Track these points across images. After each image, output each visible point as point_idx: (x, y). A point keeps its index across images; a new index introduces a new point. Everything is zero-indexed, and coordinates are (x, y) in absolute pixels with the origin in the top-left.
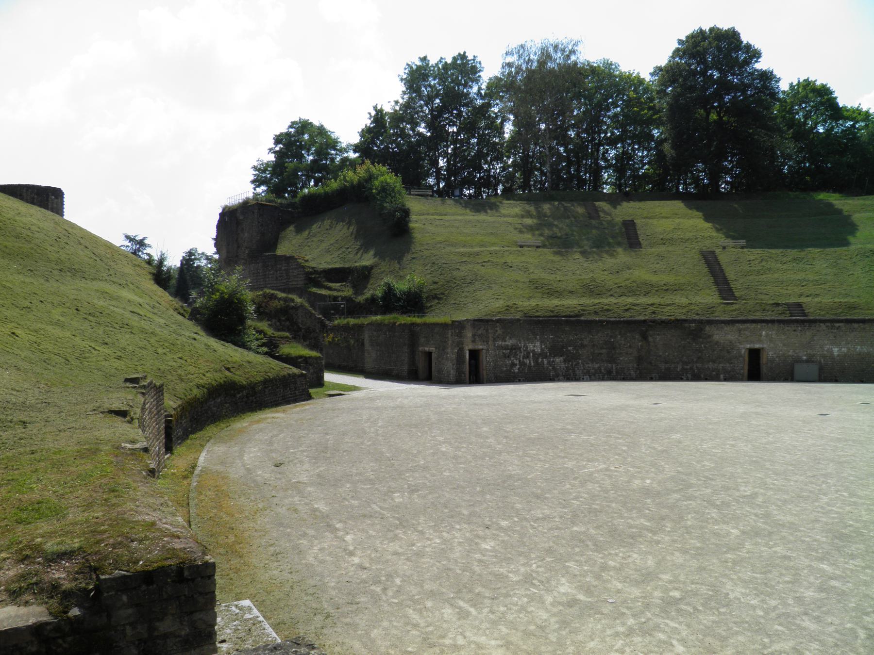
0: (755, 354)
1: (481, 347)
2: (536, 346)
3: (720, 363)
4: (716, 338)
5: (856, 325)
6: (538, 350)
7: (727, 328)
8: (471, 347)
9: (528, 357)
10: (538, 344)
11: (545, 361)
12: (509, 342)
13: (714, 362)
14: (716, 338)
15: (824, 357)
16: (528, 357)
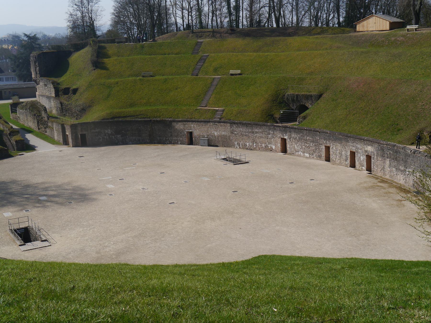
0: (191, 133)
1: (85, 133)
2: (109, 131)
3: (178, 137)
4: (176, 127)
5: (222, 124)
6: (110, 132)
7: (180, 123)
8: (81, 133)
9: (106, 135)
10: (109, 130)
11: (113, 137)
12: (97, 130)
13: (176, 137)
14: (176, 127)
15: (212, 136)
16: (106, 135)
